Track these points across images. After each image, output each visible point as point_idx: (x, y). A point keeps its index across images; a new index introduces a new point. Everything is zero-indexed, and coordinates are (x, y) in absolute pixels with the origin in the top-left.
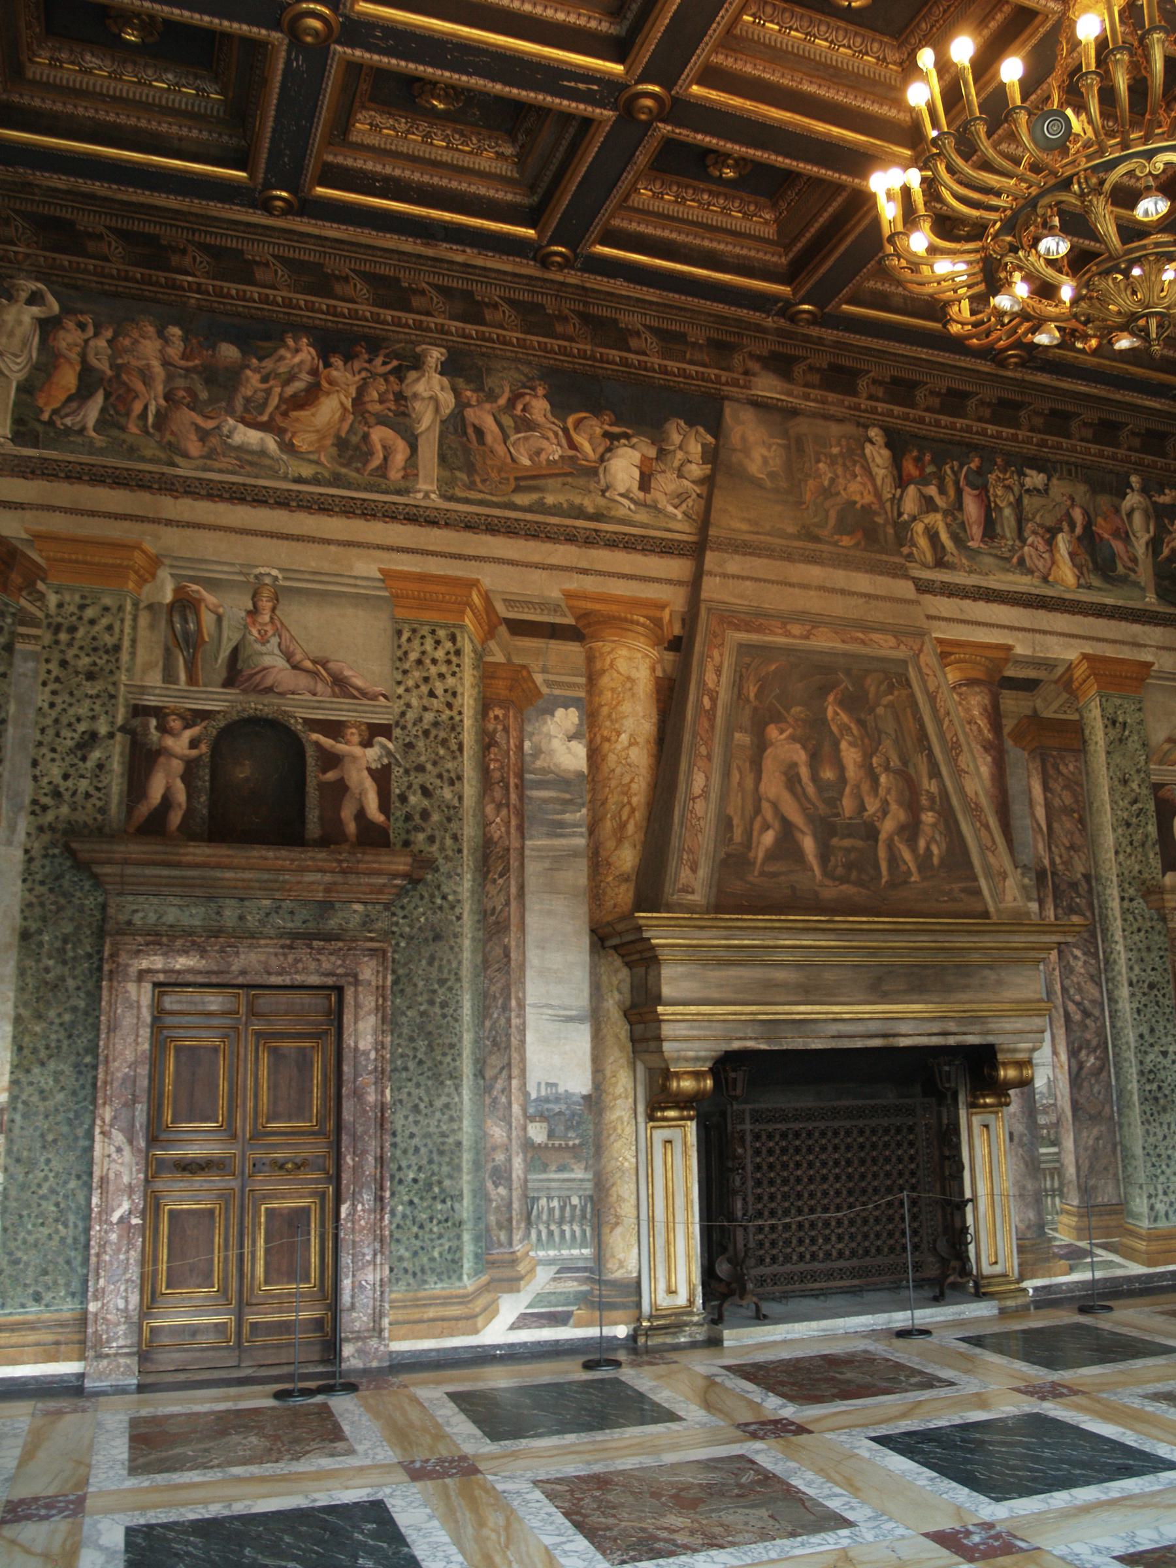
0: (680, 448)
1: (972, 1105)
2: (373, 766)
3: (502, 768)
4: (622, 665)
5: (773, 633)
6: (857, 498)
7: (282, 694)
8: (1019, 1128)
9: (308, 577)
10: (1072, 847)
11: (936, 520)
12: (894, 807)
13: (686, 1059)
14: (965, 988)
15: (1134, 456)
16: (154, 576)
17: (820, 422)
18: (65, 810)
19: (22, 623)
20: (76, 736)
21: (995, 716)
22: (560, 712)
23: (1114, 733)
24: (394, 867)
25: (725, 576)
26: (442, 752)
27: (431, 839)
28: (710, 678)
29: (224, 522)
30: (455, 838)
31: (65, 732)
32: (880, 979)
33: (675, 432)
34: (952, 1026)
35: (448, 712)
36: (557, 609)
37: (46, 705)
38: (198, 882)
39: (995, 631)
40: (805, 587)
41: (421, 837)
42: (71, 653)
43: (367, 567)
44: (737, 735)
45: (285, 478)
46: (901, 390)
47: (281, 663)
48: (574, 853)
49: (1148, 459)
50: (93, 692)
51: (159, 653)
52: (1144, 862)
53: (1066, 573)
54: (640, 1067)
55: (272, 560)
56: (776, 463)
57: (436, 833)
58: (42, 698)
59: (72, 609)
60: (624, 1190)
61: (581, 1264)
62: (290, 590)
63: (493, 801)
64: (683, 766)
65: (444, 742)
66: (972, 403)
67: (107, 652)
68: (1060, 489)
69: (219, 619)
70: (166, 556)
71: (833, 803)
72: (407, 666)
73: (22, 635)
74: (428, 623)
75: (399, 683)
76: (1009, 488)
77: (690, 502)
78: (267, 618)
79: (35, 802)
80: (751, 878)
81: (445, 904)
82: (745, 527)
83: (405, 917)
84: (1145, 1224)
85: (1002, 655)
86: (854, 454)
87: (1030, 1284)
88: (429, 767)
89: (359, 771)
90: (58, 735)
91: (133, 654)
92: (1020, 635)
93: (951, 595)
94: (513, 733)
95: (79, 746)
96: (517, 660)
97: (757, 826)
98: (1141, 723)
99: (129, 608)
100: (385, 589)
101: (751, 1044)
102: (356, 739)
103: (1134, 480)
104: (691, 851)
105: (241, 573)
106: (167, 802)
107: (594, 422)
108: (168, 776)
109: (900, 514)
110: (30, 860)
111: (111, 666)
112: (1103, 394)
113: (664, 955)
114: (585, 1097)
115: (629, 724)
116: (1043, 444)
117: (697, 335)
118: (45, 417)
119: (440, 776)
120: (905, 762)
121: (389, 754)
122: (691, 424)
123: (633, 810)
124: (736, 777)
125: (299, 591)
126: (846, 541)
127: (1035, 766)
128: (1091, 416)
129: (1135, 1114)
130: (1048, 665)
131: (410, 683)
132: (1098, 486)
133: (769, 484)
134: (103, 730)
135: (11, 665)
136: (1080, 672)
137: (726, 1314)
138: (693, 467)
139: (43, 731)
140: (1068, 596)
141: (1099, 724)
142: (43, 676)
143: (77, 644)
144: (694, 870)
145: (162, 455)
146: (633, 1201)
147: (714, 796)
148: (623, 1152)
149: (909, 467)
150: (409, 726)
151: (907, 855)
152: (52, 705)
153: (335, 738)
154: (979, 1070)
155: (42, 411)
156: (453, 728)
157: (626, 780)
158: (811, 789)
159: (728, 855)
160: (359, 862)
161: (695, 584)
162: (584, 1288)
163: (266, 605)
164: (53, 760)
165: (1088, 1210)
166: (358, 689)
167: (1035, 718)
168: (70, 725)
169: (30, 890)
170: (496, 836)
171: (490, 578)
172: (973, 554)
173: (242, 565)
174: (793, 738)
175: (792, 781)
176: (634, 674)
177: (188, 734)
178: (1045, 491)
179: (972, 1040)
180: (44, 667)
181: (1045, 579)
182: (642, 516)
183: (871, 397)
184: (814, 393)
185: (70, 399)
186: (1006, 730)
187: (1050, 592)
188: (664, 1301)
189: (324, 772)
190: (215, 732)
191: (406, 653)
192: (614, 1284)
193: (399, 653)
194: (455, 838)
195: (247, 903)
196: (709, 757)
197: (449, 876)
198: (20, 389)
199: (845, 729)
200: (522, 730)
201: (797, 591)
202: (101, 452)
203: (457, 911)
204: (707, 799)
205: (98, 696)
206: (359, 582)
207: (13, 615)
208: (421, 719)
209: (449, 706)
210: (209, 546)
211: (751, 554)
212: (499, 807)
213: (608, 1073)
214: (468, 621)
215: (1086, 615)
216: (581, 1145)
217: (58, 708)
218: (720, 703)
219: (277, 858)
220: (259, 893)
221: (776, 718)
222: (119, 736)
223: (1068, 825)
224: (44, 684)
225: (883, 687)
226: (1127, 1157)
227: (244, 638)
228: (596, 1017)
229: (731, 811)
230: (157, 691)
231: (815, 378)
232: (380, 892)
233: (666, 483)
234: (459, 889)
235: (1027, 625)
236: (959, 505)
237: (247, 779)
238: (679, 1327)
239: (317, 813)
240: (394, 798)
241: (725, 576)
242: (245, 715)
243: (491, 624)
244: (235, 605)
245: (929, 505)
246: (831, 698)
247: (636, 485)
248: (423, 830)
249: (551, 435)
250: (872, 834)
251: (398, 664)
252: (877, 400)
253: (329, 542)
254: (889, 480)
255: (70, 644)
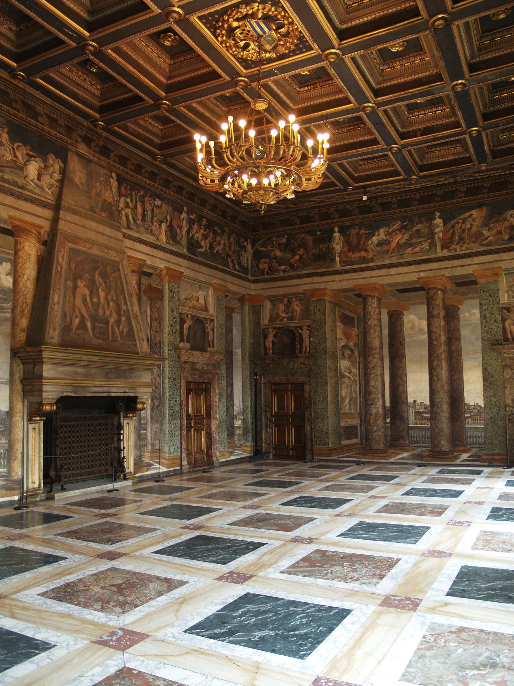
0: (52, 166)
1: (126, 417)
4: (27, 248)
5: (80, 245)
6: (107, 199)
8: (137, 424)
10: (157, 332)
11: (128, 211)
12: (114, 314)
13: (49, 399)
14: (131, 377)
15: (186, 200)
17: (98, 166)
21: (139, 284)
22: (4, 264)
23: (171, 294)
25: (66, 221)
28: (60, 259)
32: (108, 373)
33: (51, 159)
34: (127, 390)
36: (6, 222)
39: (142, 254)
40: (91, 229)
44: (68, 282)
46: (123, 160)
48: (6, 320)
49: (190, 202)
52: (175, 339)
53: (163, 237)
54: (26, 401)
56: (84, 180)
60: (19, 447)
61: (3, 474)
64: (51, 292)
66: (143, 170)
68: (165, 207)
71: (96, 310)
76: (150, 204)
77: (54, 188)
80: (71, 335)
82: (73, 203)
84: (168, 455)
85: (143, 263)
86: (107, 182)
87: (137, 475)
92: (149, 257)
93: (130, 239)
97: (74, 316)
98: (178, 292)
101: (69, 394)
103: (185, 208)
104: (53, 324)
107: (23, 148)
109: (118, 207)
112: (180, 176)
113: (45, 360)
114: (7, 413)
115: (27, 272)
116: (162, 190)
117: (62, 122)
120: (117, 298)
122: (57, 157)
123: (27, 305)
124: (68, 298)
126: (104, 215)
127: (149, 303)
128: (176, 183)
129: (167, 420)
130: (155, 268)
132: (175, 209)
133: (81, 187)
136: (164, 272)
137: (53, 489)
138: (56, 175)
140: (163, 245)
141: (167, 291)
144: (54, 331)
146: (21, 451)
147: (61, 304)
148: (18, 433)
149: (123, 190)
151: (117, 331)
154: (130, 405)
157: (25, 293)
158: (90, 305)
159: (65, 326)
161: (55, 221)
162: (4, 483)
165: (153, 451)
167: (150, 287)
172: (138, 225)
174: (85, 286)
175: (84, 301)
176: (31, 253)
178: (160, 207)
179: (132, 395)
181: (157, 238)
182: (37, 191)
183: (114, 161)
184: (97, 155)
186: (142, 290)
187: (158, 243)
188: (31, 486)
192: (14, 481)
196: (59, 289)
199: (101, 284)
201: (88, 231)
204: (59, 305)
211: (75, 214)
213: (15, 404)
215: (167, 253)
216: (5, 430)
218: (63, 269)
221: (81, 277)
223: (156, 324)
225: (112, 271)
226: (164, 434)
228: (11, 382)
229: (66, 310)
231: (98, 149)
233: (46, 179)
235: (151, 254)
236: (136, 207)
238: (37, 495)
241: (66, 221)
245: (127, 205)
246: (97, 272)
247: (36, 177)
249: (8, 150)
250: (107, 323)
252: (116, 162)
254: (116, 194)
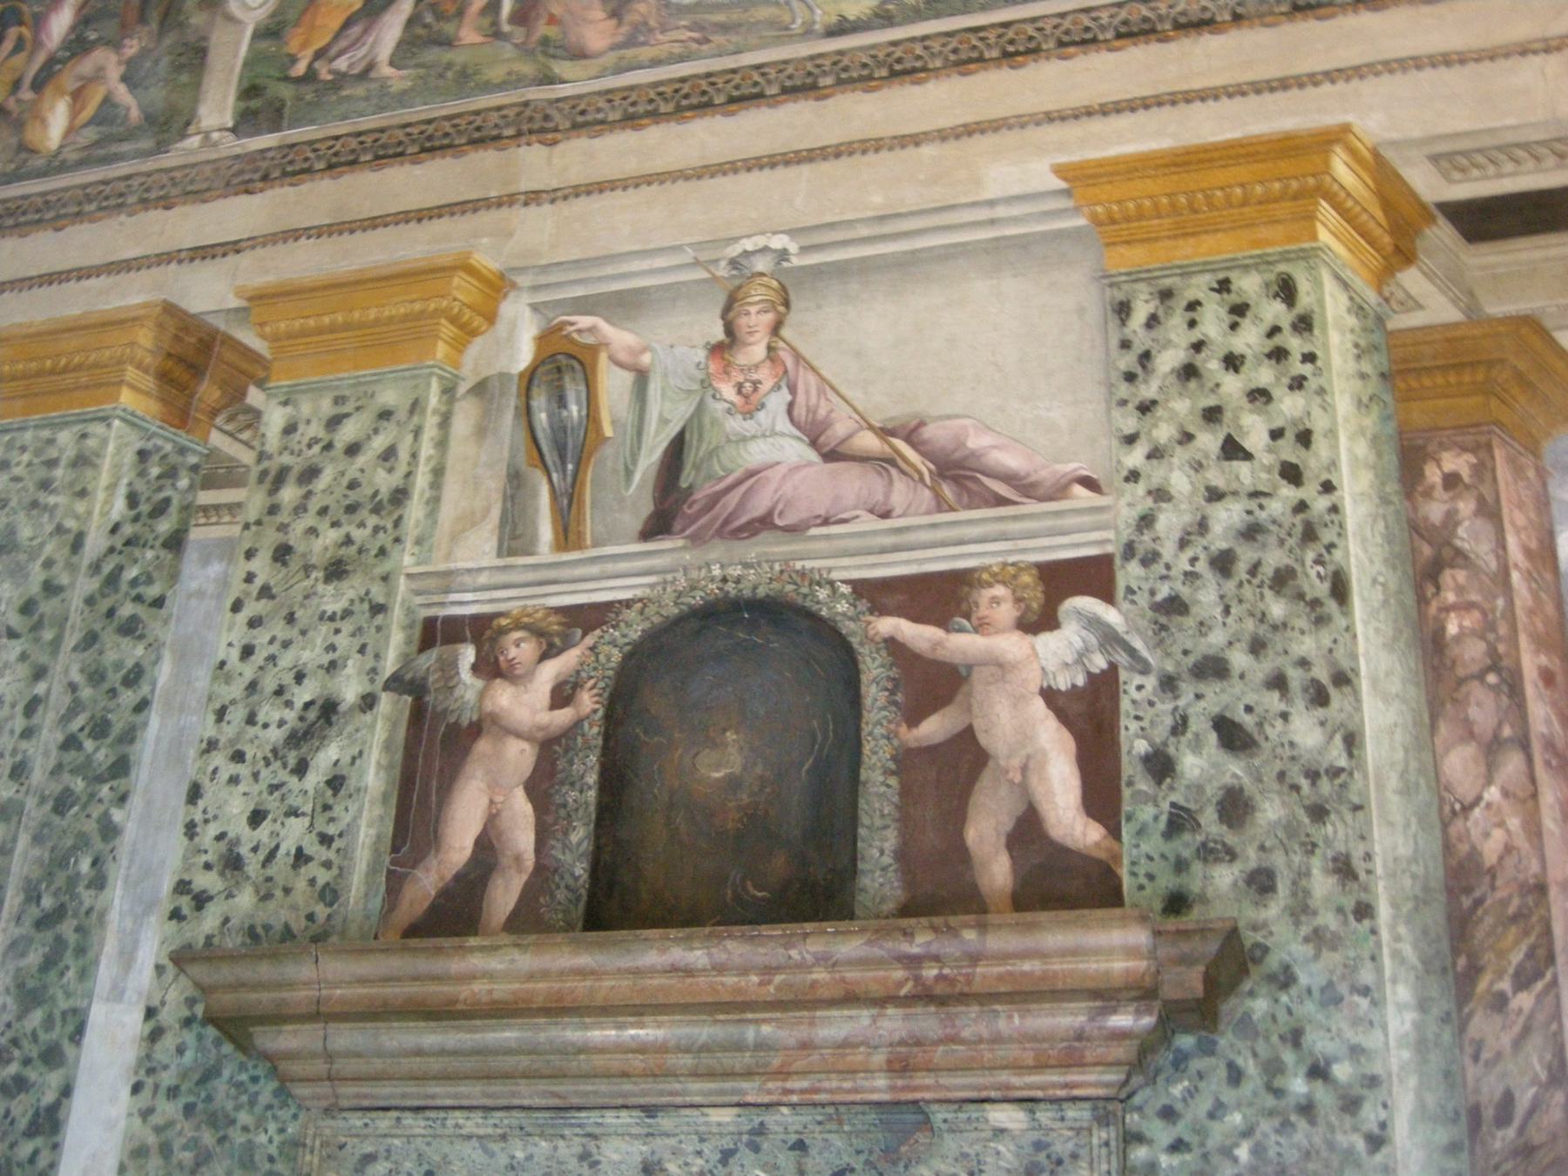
2: (1063, 683)
3: (1490, 626)
7: (794, 530)
9: (864, 232)
16: (491, 318)
18: (245, 899)
19: (209, 483)
20: (291, 715)
24: (1092, 966)
26: (1277, 609)
27: (1261, 883)
29: (658, 165)
30: (1344, 869)
31: (270, 712)
35: (1288, 492)
37: (235, 654)
38: (524, 1062)
41: (1225, 877)
42: (300, 526)
43: (1021, 172)
45: (808, 33)
47: (795, 450)
50: (332, 607)
51: (494, 485)
55: (764, 217)
57: (1278, 860)
58: (227, 637)
59: (316, 430)
62: (817, 271)
63: (1469, 734)
65: (1282, 580)
67: (377, 510)
69: (642, 377)
70: (522, 270)
72: (1149, 390)
73: (205, 509)
74: (1206, 268)
75: (1131, 440)
78: (758, 351)
79: (182, 887)
81: (1324, 1096)
83: (1177, 1146)
88: (1239, 659)
89: (1018, 700)
90: (251, 720)
91: (434, 502)
94: (1516, 518)
95: (296, 739)
96: (1496, 308)
99: (434, 399)
100: (1077, 210)
102: (1007, 612)
105: (696, 263)
106: (487, 849)
108: (493, 785)
110: (155, 1035)
111: (384, 539)
118: (300, 68)
119: (1278, 682)
121: (1109, 638)
125: (840, 270)
131: (1164, 433)
134: (350, 689)
135: (174, 577)
139: (221, 714)
142: (237, 588)
143: (314, 505)
145: (527, 69)
150: (1168, 550)
152: (247, 651)
153: (943, 622)
155: (294, 60)
156: (1309, 534)
160: (975, 958)
163: (756, 320)
164: (234, 780)
166: (1009, 478)
168: (279, 692)
169: (146, 1114)
170: (1490, 850)
171: (1379, 115)
173: (697, 246)
177: (551, 671)
180: (243, 567)
185: (347, 24)
189: (914, 719)
190: (617, 656)
191: (1146, 357)
193: (1127, 361)
194: (1344, 869)
195: (665, 1122)
197: (1330, 998)
198: (259, 35)
200: (1543, 503)
202: (403, 99)
203: (1370, 1115)
205: (347, 613)
206: (1001, 212)
207: (194, 468)
208: (1203, 526)
209: (1292, 474)
210: (617, 224)
212: (1492, 749)
214: (1329, 233)
217: (259, 658)
219: (720, 969)
220: (697, 1089)
222: (386, 702)
224: (237, 607)
227: (700, 408)
230: (483, 579)
232: (1071, 1060)
234: (1373, 1040)
237: (733, 783)
239: (891, 839)
240: (1130, 767)
242: (697, 599)
243: (1398, 231)
244: (677, 341)
248: (1232, 855)
251: (1124, 390)
253: (916, 140)
255: (300, 509)
